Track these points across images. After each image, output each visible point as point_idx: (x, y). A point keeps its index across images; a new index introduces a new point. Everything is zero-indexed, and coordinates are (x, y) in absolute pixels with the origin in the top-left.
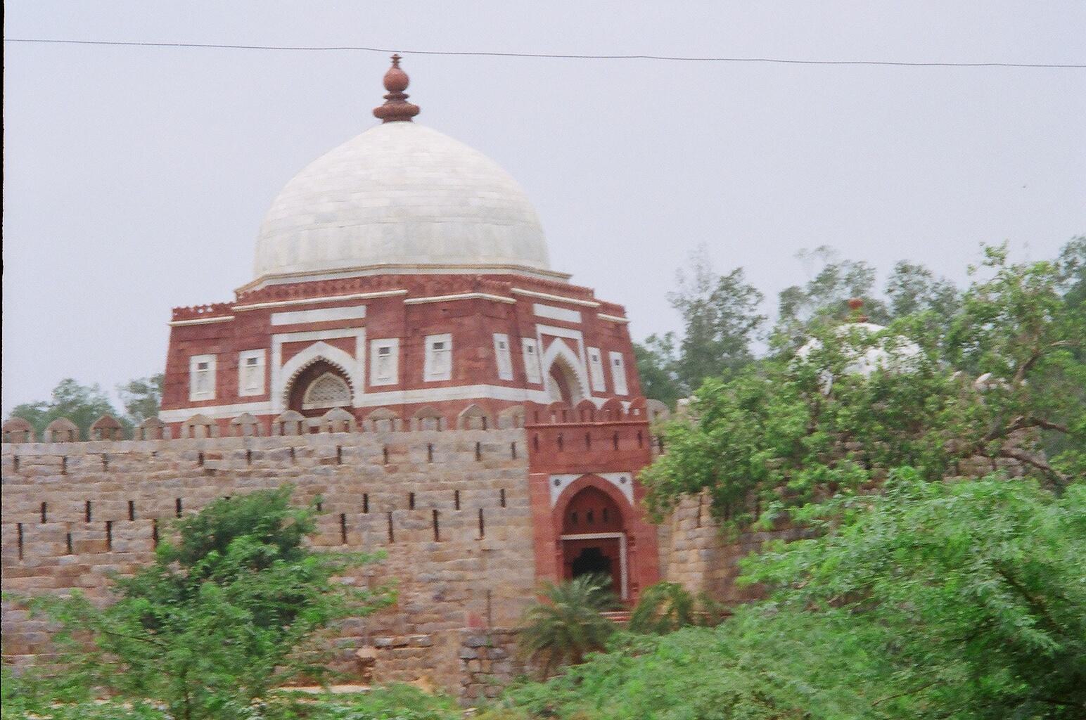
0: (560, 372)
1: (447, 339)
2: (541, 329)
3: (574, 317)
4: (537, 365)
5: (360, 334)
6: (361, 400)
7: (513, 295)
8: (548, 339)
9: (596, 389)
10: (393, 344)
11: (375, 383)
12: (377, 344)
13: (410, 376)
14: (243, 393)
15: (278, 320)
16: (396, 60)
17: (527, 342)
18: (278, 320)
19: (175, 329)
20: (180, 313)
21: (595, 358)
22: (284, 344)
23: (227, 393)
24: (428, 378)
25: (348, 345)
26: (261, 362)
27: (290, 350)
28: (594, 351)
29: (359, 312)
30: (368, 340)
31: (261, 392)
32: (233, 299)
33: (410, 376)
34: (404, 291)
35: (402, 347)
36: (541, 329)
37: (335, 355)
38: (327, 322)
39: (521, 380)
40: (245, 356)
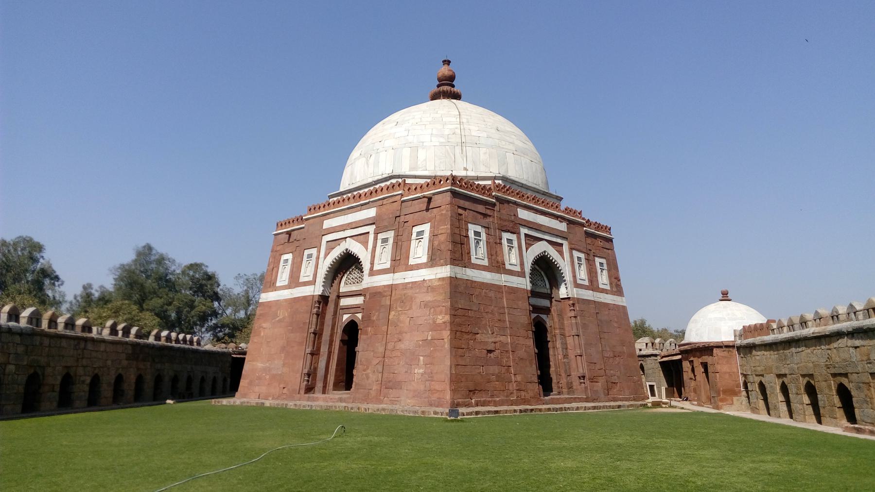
1: (426, 228)
2: (524, 231)
3: (562, 227)
4: (518, 256)
5: (371, 229)
6: (368, 282)
7: (493, 197)
8: (531, 240)
9: (579, 282)
10: (390, 235)
11: (377, 267)
12: (381, 236)
14: (302, 279)
15: (328, 224)
17: (506, 236)
20: (281, 225)
21: (579, 259)
23: (295, 281)
24: (412, 262)
28: (576, 254)
29: (371, 213)
30: (376, 234)
31: (311, 278)
32: (307, 210)
37: (356, 248)
38: (351, 223)
39: (497, 265)
40: (307, 252)
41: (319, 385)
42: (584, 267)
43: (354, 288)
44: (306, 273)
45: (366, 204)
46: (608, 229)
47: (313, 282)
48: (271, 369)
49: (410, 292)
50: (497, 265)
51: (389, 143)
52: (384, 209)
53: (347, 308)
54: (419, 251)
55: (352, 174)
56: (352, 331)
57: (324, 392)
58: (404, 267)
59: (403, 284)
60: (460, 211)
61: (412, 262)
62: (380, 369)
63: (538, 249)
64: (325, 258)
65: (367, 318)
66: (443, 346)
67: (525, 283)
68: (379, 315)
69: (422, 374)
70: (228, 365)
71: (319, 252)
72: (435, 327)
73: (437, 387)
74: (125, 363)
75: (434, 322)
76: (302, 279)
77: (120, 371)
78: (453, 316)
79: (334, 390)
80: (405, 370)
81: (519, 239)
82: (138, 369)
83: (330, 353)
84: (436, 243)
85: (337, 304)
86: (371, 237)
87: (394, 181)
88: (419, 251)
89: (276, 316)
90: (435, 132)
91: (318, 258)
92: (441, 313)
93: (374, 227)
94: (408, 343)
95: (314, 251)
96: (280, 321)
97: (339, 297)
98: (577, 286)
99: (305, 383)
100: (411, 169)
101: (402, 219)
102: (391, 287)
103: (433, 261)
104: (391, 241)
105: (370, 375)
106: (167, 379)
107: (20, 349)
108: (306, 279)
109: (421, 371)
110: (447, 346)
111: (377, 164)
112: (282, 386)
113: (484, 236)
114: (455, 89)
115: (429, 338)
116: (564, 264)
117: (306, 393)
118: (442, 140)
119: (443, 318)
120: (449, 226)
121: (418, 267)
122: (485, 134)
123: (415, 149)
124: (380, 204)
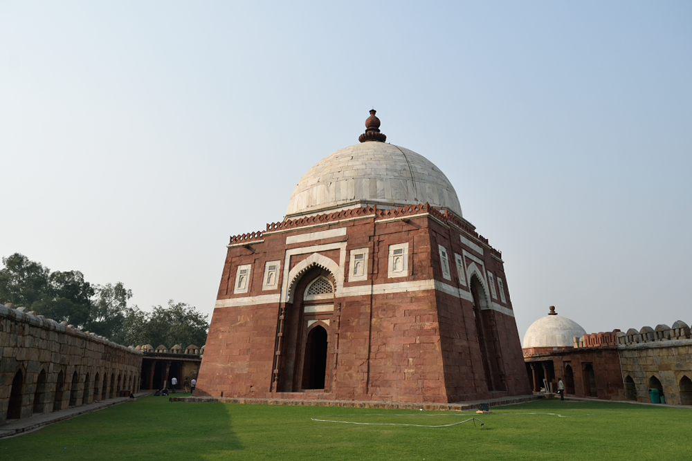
0: (475, 284)
1: (405, 247)
2: (464, 252)
3: (480, 251)
6: (341, 291)
8: (469, 261)
10: (365, 252)
12: (353, 252)
13: (377, 272)
15: (290, 240)
16: (373, 112)
17: (457, 256)
18: (290, 240)
19: (230, 248)
20: (234, 239)
22: (291, 256)
23: (255, 289)
25: (333, 255)
26: (279, 267)
27: (294, 260)
29: (342, 232)
33: (377, 272)
34: (374, 215)
35: (370, 254)
36: (464, 252)
37: (325, 262)
39: (455, 282)
41: (290, 383)
42: (494, 284)
43: (319, 297)
44: (270, 283)
45: (334, 224)
46: (499, 255)
47: (280, 291)
48: (233, 370)
49: (392, 302)
50: (455, 282)
51: (348, 173)
52: (355, 229)
53: (313, 315)
54: (398, 264)
55: (310, 197)
56: (319, 335)
57: (293, 391)
58: (383, 280)
59: (383, 295)
60: (434, 234)
61: (391, 275)
62: (366, 370)
63: (472, 268)
64: (290, 269)
65: (343, 324)
66: (434, 349)
67: (468, 296)
68: (358, 322)
69: (413, 374)
70: (141, 365)
71: (283, 264)
72: (421, 332)
73: (431, 384)
74: (101, 361)
75: (422, 328)
76: (266, 287)
77: (98, 370)
78: (440, 323)
79: (302, 388)
80: (392, 370)
81: (462, 257)
82: (105, 368)
83: (298, 355)
84: (416, 260)
85: (302, 309)
86: (343, 254)
87: (359, 206)
88: (398, 264)
89: (235, 321)
90: (388, 167)
91: (282, 270)
92: (428, 320)
93: (346, 244)
94: (394, 346)
95: (278, 264)
96: (241, 325)
97: (304, 304)
98: (493, 300)
99: (276, 382)
100: (371, 197)
101: (376, 239)
102: (372, 297)
103: (414, 274)
104: (366, 257)
105: (354, 375)
106: (116, 378)
107: (56, 348)
108: (270, 288)
109: (412, 371)
110: (438, 348)
111: (337, 190)
112: (249, 385)
113: (446, 254)
114: (381, 133)
115: (418, 342)
116: (484, 282)
117: (277, 392)
118: (397, 175)
119: (431, 324)
120: (429, 246)
121: (399, 280)
122: (426, 173)
123: (373, 180)
124: (351, 226)
